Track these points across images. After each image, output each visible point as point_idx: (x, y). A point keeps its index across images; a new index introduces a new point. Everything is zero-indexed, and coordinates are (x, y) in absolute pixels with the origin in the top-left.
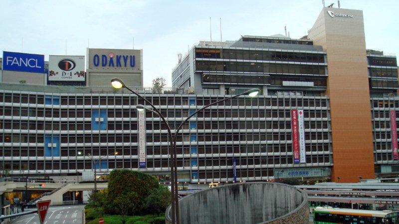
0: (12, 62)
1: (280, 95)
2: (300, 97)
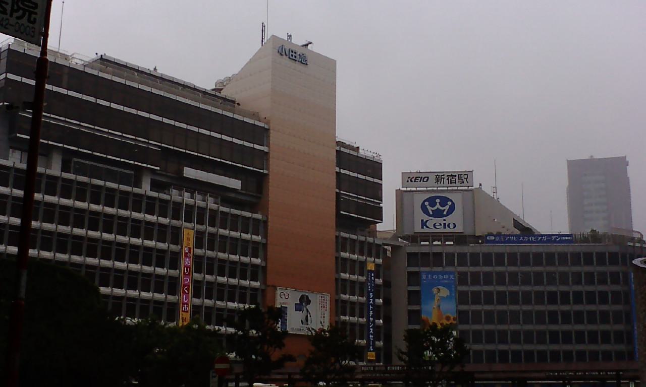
1: (175, 195)
2: (214, 206)
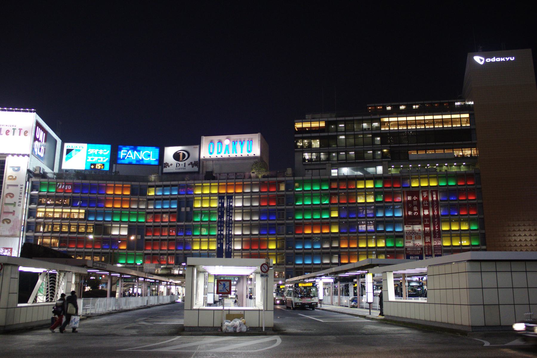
0: (126, 156)
